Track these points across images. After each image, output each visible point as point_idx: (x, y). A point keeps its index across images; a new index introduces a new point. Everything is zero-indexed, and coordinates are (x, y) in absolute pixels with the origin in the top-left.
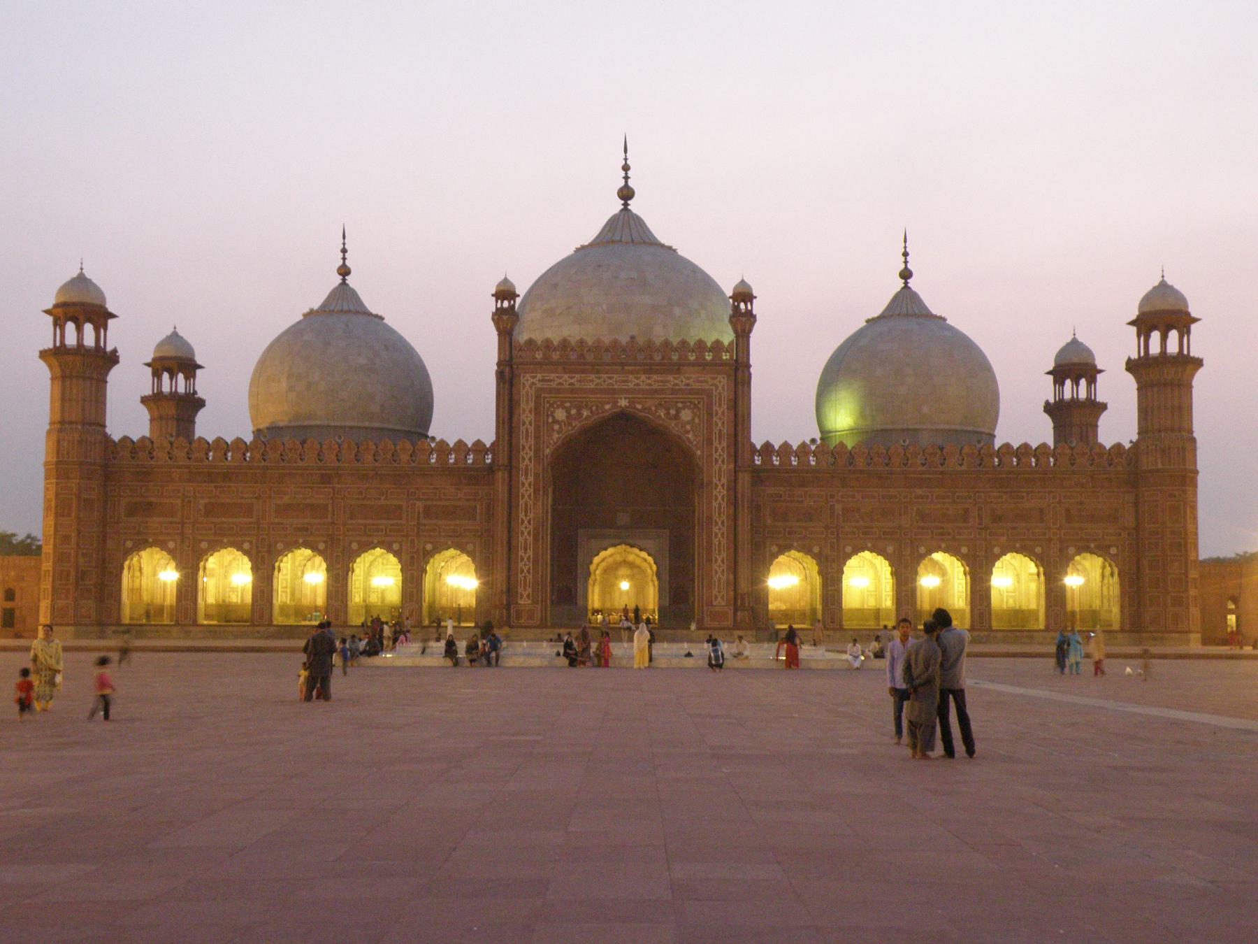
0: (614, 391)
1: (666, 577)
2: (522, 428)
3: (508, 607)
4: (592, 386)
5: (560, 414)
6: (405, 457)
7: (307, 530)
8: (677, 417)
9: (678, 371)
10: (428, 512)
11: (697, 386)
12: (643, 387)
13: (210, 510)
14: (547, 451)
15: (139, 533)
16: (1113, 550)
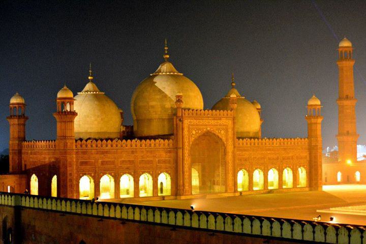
0: (206, 125)
1: (201, 178)
2: (185, 136)
3: (183, 190)
4: (201, 124)
5: (194, 132)
6: (153, 145)
7: (128, 168)
8: (220, 133)
9: (220, 119)
10: (159, 162)
11: (225, 124)
12: (213, 124)
13: (103, 163)
14: (191, 143)
15: (83, 171)
16: (305, 166)
